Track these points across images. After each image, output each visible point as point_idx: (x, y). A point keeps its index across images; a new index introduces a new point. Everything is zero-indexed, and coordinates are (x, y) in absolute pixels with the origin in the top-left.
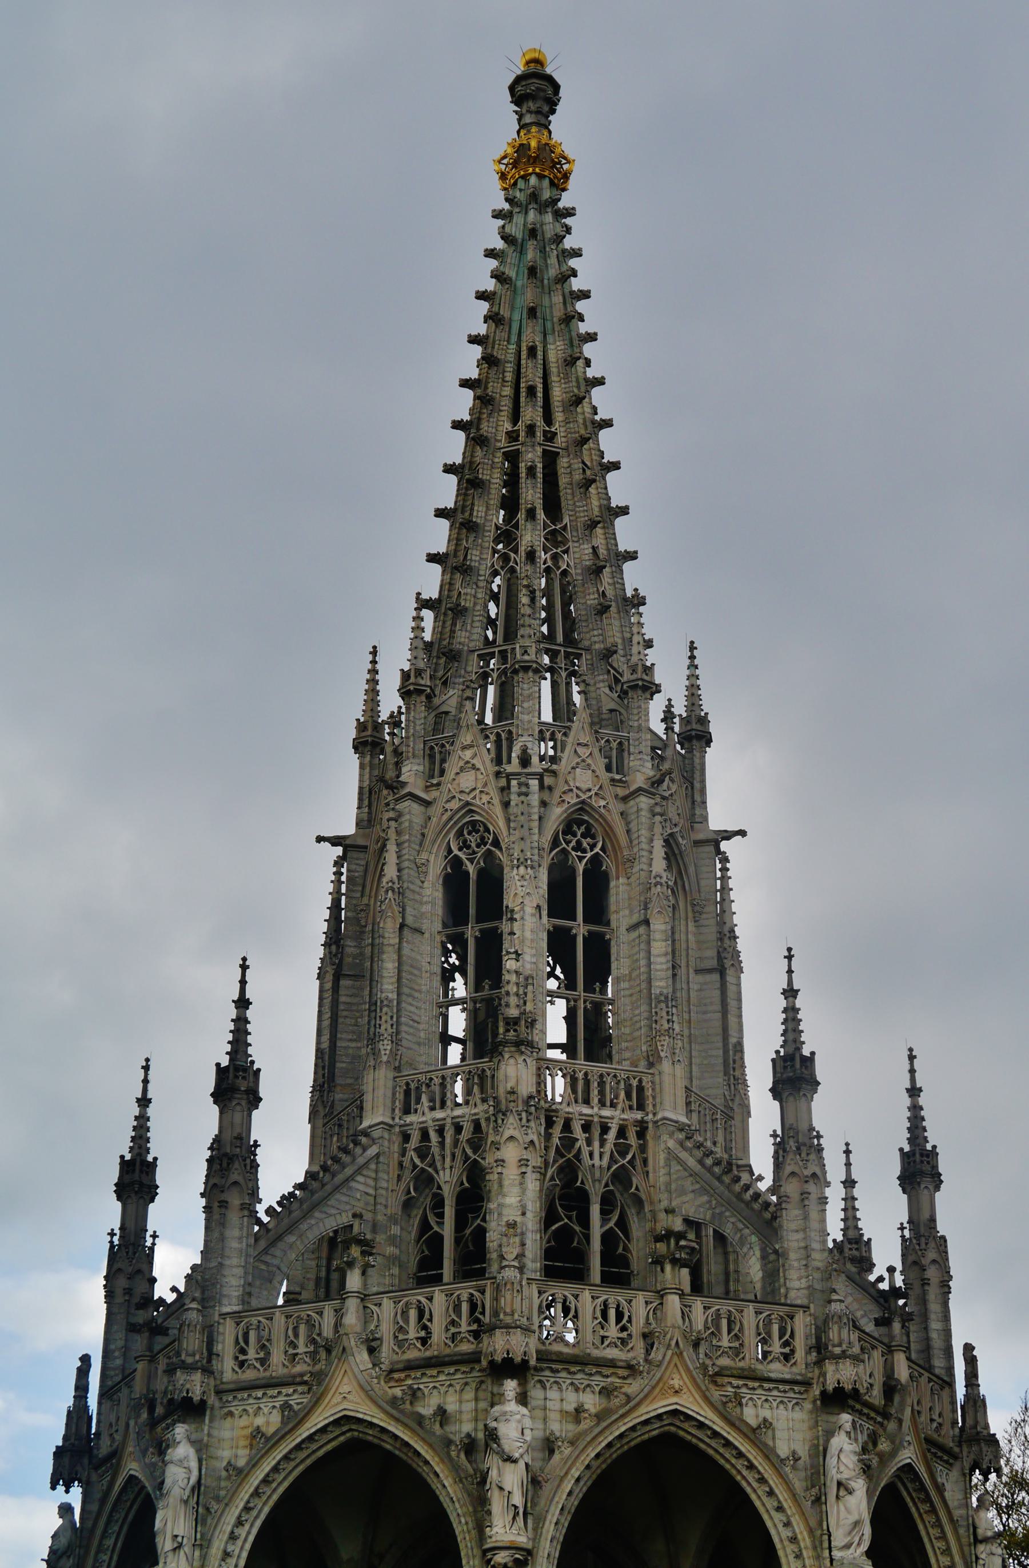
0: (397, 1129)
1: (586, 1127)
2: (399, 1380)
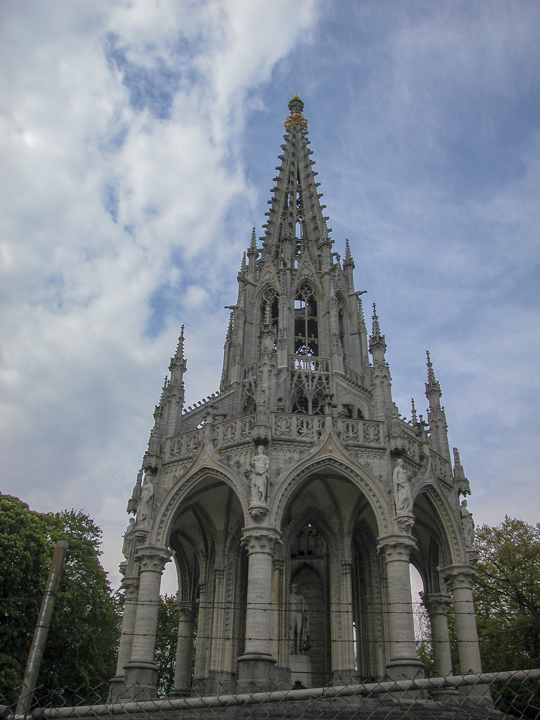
0: (241, 384)
1: (307, 377)
2: (224, 453)
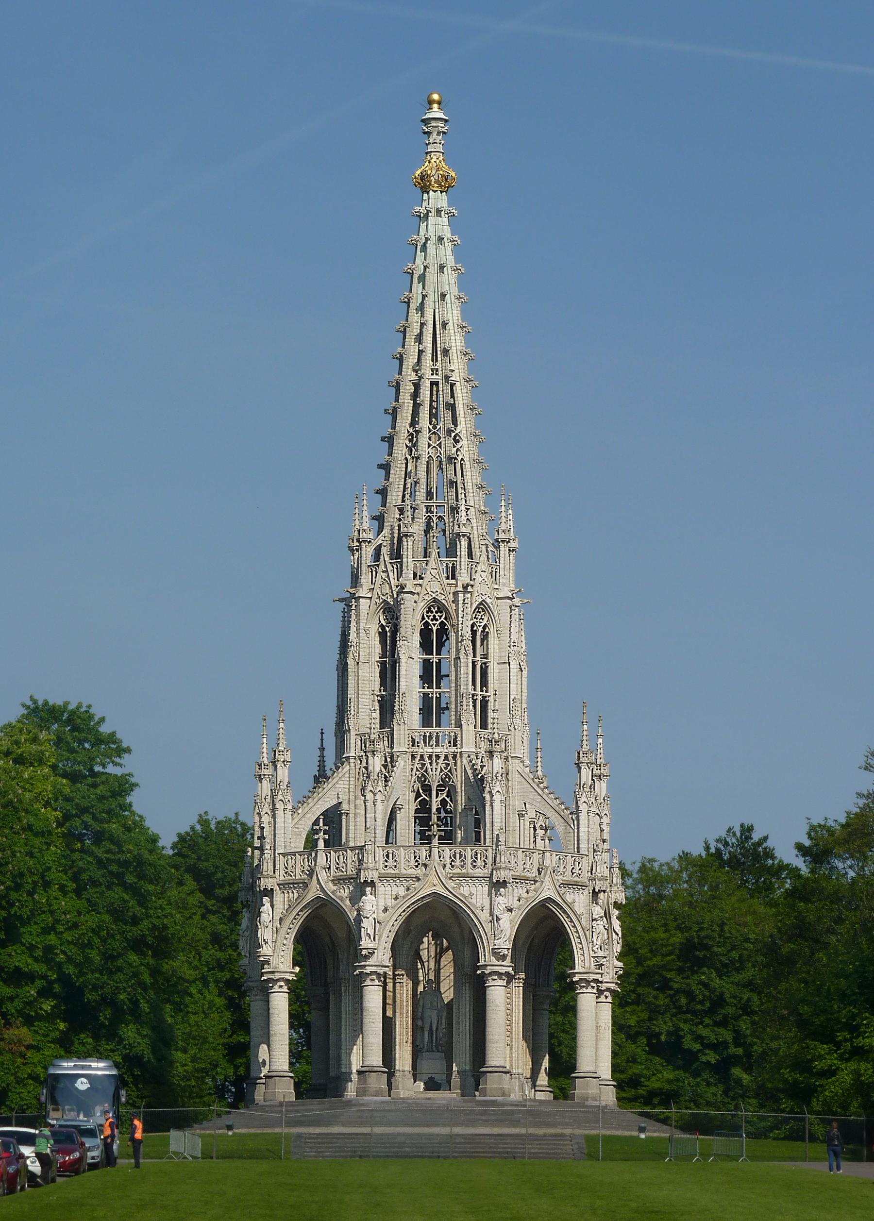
1: (430, 757)
